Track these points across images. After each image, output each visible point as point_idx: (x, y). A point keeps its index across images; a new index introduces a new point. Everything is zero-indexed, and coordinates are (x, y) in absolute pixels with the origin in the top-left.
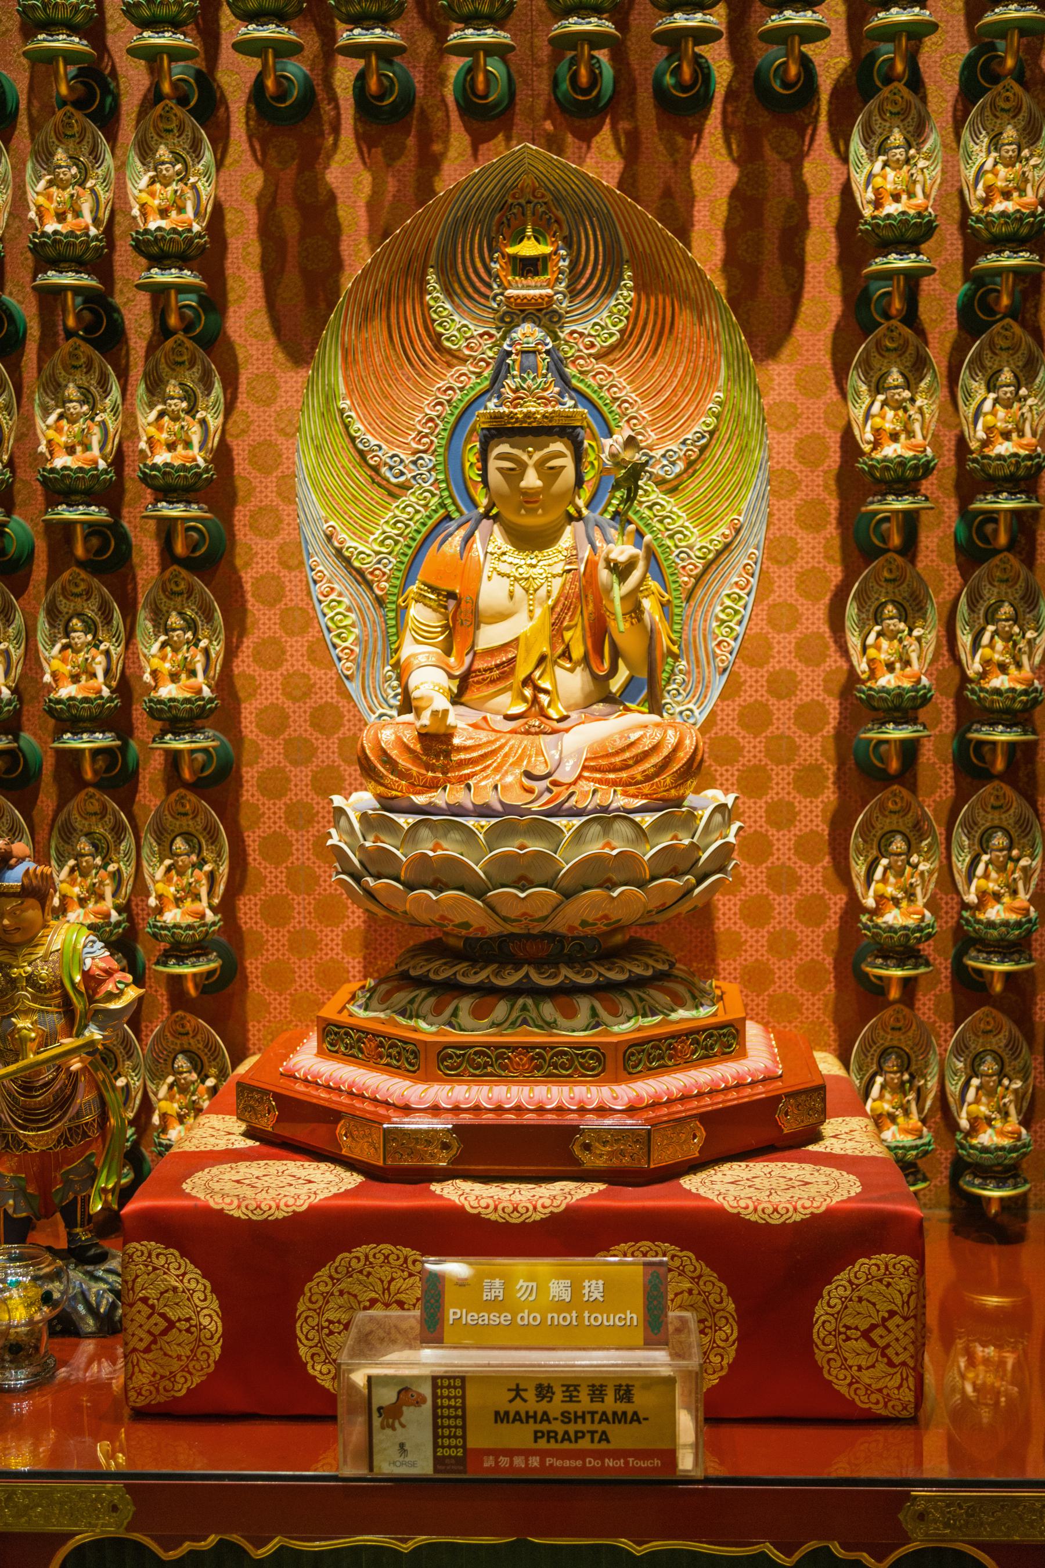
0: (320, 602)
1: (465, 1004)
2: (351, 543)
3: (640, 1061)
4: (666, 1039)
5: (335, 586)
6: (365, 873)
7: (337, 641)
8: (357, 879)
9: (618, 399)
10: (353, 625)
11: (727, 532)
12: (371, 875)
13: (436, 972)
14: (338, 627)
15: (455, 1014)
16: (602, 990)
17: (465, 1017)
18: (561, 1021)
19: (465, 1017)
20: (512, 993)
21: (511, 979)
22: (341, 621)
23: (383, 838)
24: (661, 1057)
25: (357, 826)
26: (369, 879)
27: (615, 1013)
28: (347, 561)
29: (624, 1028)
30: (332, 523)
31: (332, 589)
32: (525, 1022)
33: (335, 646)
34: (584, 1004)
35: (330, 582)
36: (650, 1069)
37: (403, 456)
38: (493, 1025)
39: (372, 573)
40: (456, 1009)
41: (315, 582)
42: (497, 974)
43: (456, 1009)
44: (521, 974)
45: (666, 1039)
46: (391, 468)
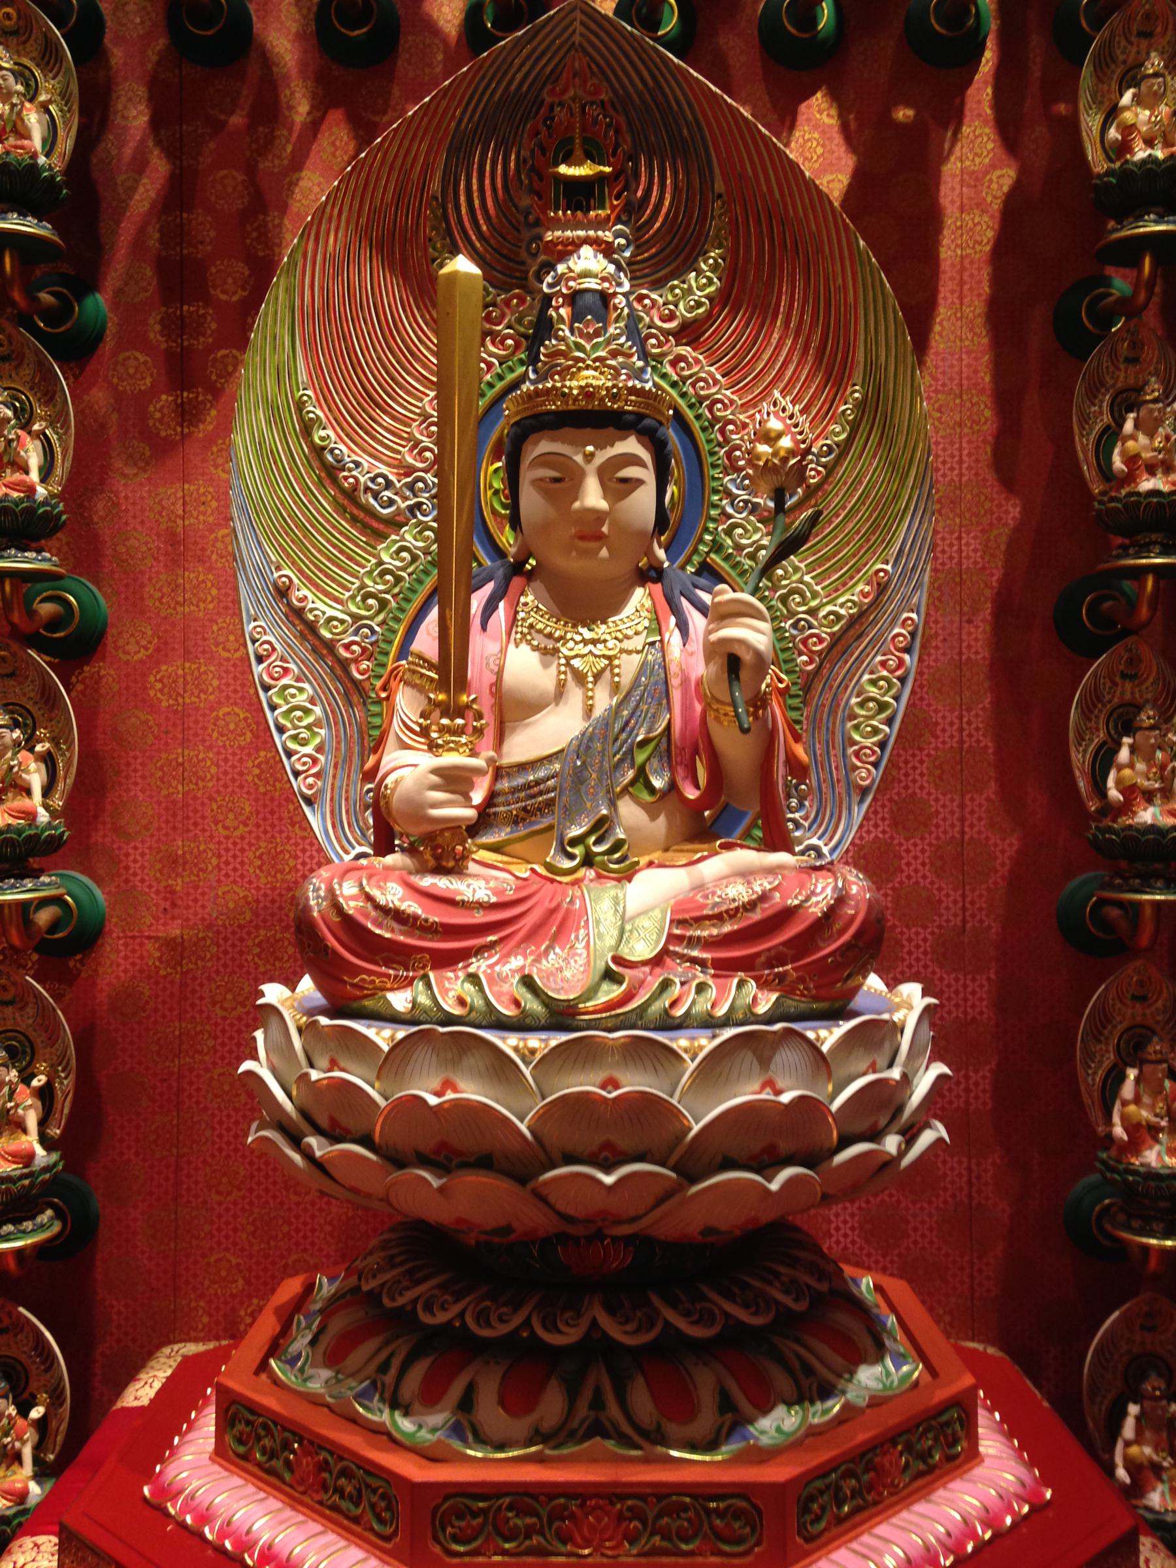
0: (267, 688)
2: (320, 608)
5: (292, 666)
7: (292, 745)
8: (296, 1141)
9: (707, 397)
10: (317, 723)
11: (867, 589)
12: (319, 1131)
14: (296, 727)
15: (466, 1404)
16: (732, 1344)
22: (300, 719)
23: (342, 1064)
26: (313, 1141)
28: (312, 627)
30: (287, 572)
31: (286, 671)
33: (289, 754)
34: (705, 1382)
35: (283, 659)
37: (391, 477)
39: (347, 647)
41: (260, 659)
46: (376, 495)
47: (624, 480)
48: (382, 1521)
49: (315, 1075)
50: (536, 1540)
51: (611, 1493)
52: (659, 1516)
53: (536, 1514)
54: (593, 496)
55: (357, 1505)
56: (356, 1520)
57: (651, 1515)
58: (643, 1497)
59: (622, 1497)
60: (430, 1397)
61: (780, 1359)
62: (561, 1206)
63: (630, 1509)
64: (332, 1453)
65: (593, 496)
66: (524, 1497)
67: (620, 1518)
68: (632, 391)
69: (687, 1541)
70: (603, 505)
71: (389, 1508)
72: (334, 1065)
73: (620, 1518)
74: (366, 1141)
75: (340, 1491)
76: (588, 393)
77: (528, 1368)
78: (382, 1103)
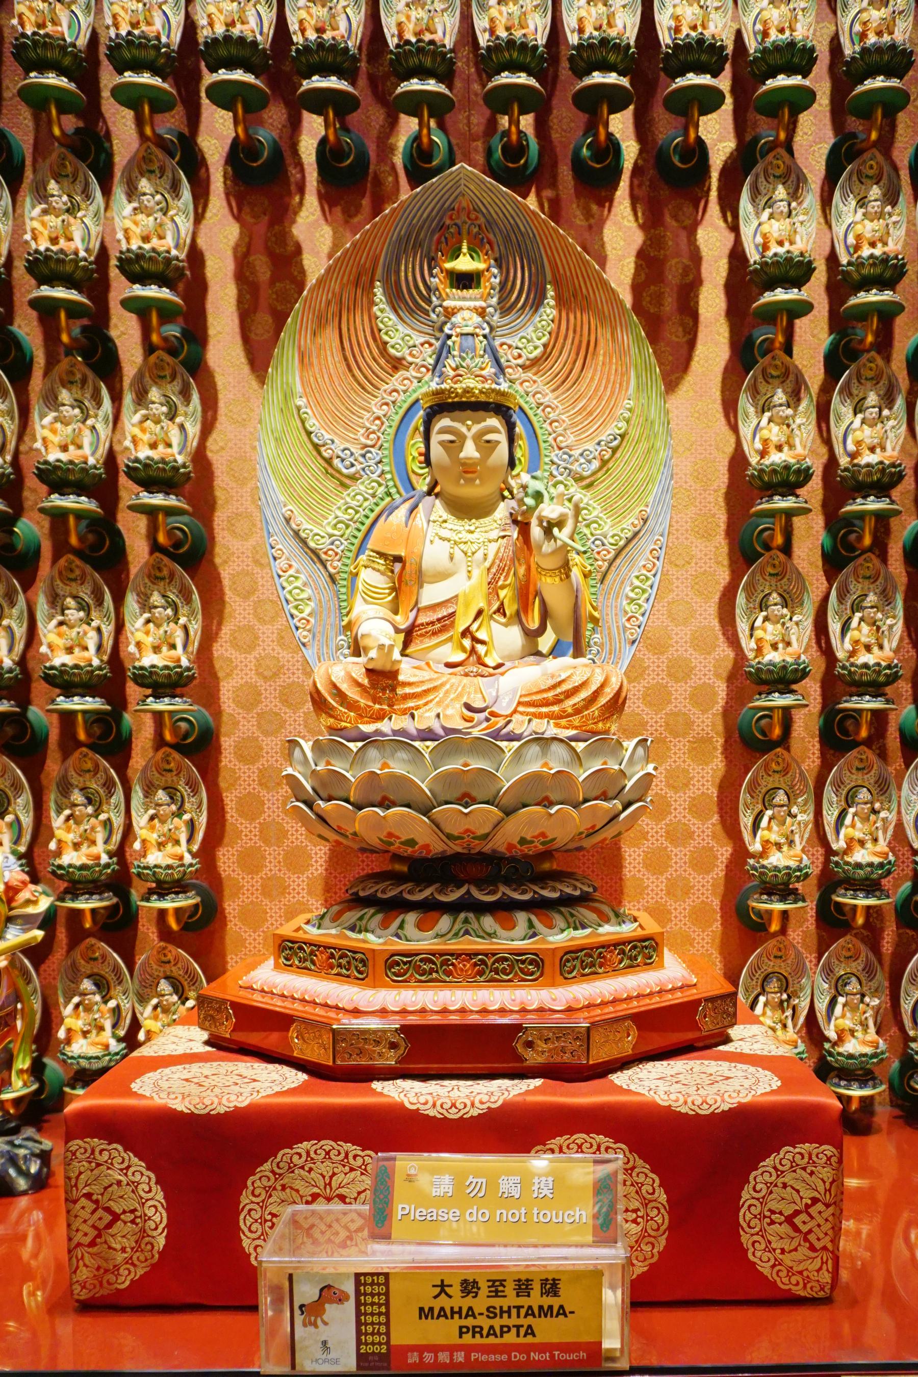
1: (411, 918)
3: (574, 967)
4: (597, 948)
6: (316, 797)
13: (384, 892)
15: (401, 927)
17: (410, 929)
18: (500, 932)
19: (410, 929)
20: (453, 909)
21: (453, 896)
24: (592, 965)
25: (309, 754)
26: (320, 802)
27: (551, 927)
29: (560, 937)
32: (467, 932)
34: (521, 917)
36: (583, 975)
38: (437, 936)
40: (403, 922)
42: (440, 892)
43: (403, 922)
44: (463, 891)
45: (597, 948)
47: (488, 442)
48: (360, 972)
49: (318, 768)
50: (434, 975)
51: (471, 955)
52: (494, 963)
53: (434, 963)
54: (470, 451)
55: (348, 970)
56: (348, 976)
57: (489, 964)
58: (486, 955)
59: (477, 954)
60: (385, 925)
61: (561, 913)
62: (448, 831)
63: (480, 960)
64: (334, 949)
65: (470, 451)
66: (430, 957)
67: (475, 965)
68: (493, 390)
69: (507, 975)
70: (477, 455)
71: (364, 965)
72: (328, 763)
73: (475, 965)
74: (347, 801)
75: (340, 966)
76: (467, 391)
77: (430, 909)
78: (353, 780)
